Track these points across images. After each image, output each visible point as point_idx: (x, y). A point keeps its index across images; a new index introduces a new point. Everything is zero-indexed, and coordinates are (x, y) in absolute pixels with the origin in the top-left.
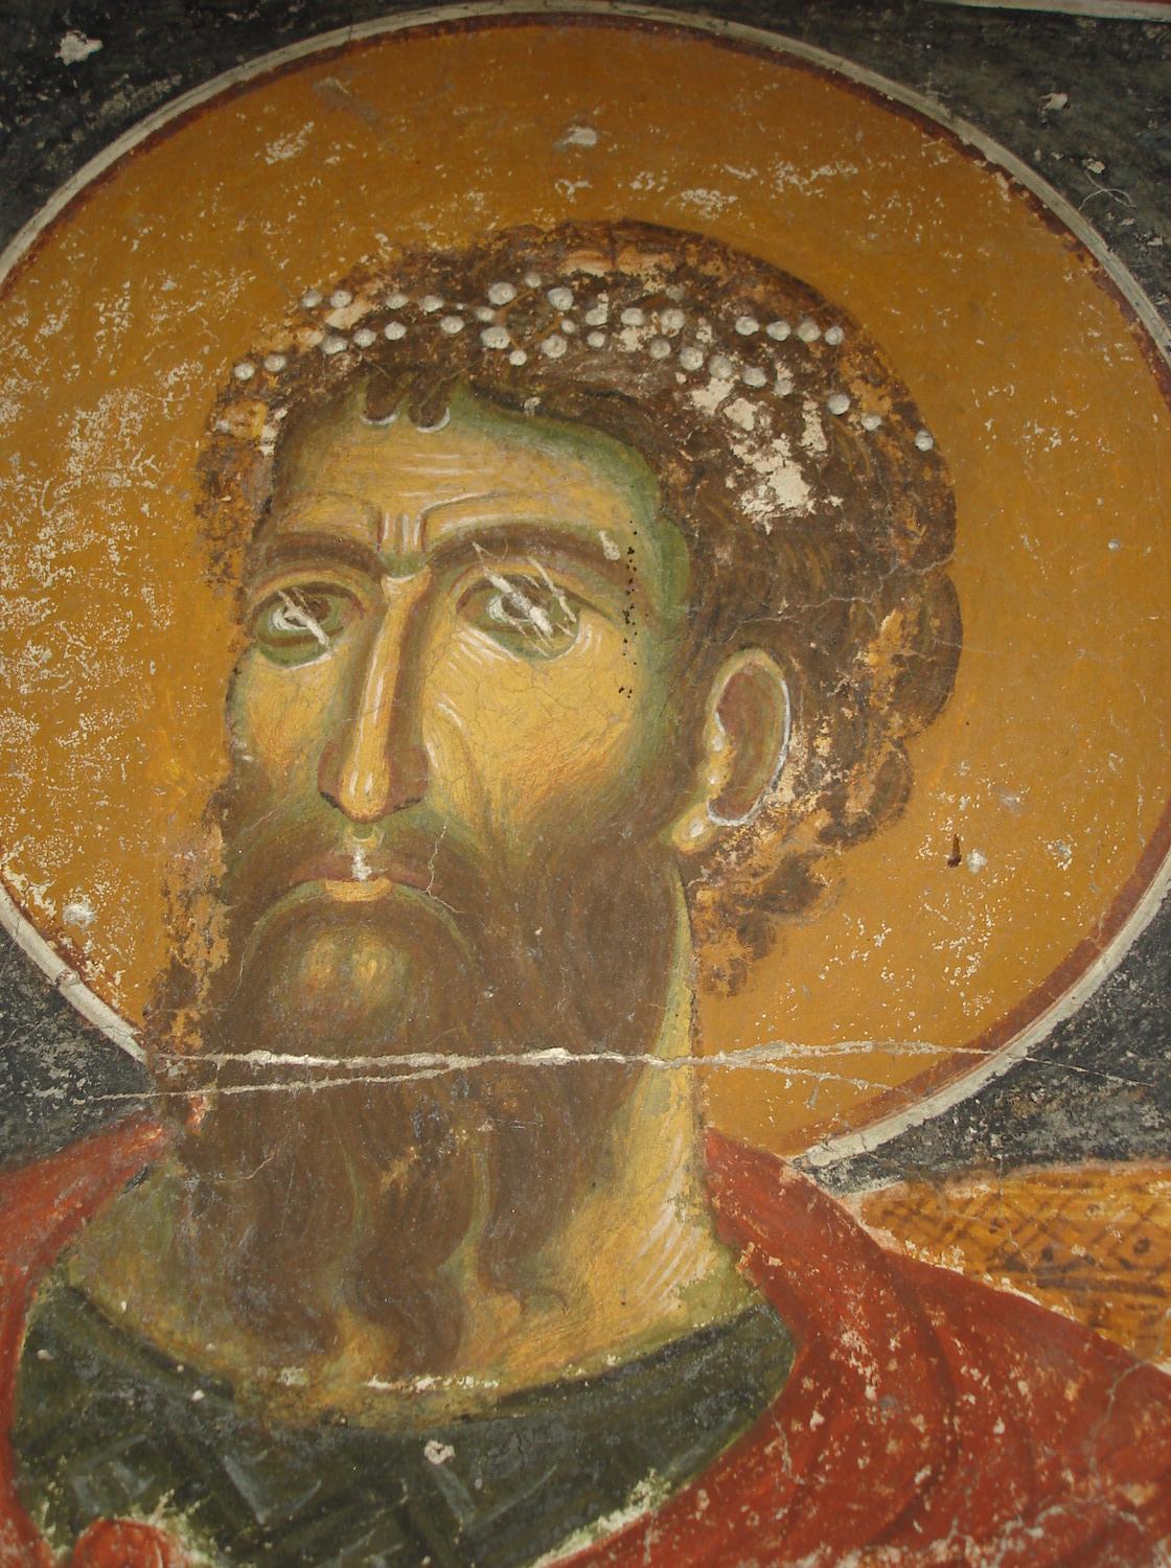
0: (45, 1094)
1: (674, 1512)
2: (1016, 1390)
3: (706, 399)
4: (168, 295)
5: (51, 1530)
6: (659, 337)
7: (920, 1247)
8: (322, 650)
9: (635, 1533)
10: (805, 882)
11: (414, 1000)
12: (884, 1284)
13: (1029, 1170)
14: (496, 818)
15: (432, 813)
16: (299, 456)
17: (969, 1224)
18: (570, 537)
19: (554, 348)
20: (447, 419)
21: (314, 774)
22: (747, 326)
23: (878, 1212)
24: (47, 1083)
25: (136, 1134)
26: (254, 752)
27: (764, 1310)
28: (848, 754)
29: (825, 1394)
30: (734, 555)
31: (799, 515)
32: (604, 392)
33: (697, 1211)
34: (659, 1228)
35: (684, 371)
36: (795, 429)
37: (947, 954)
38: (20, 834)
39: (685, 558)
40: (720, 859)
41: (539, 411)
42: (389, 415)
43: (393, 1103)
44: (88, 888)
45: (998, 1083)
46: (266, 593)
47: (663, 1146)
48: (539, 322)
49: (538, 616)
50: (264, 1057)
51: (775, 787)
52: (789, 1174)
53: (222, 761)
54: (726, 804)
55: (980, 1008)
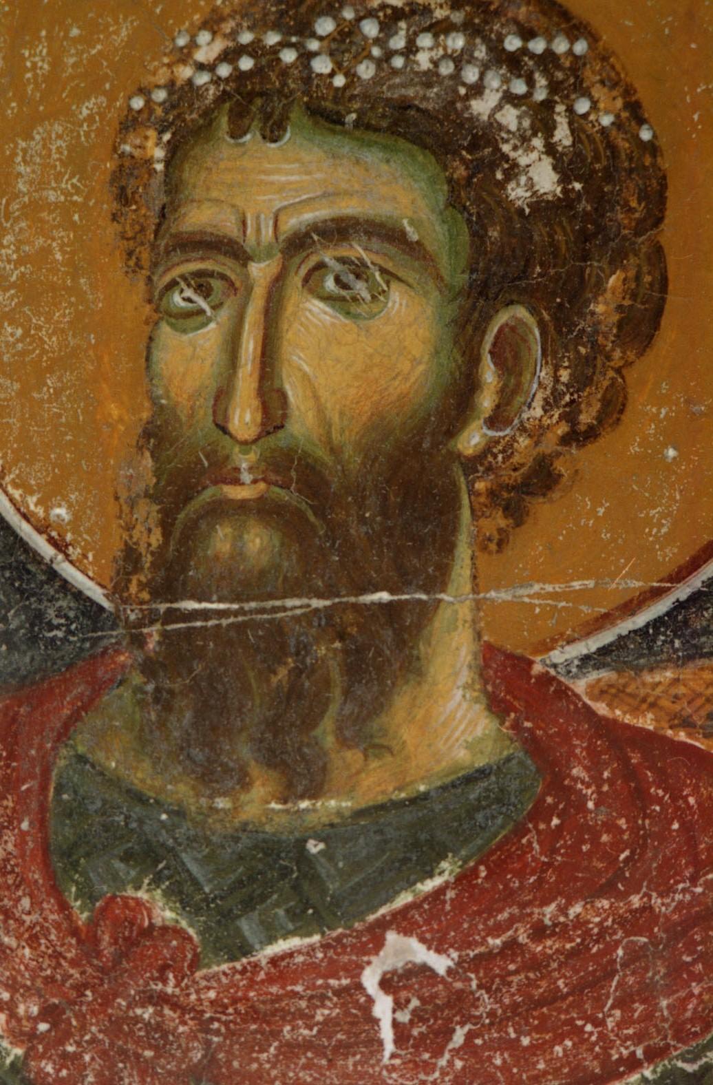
0: (51, 634)
1: (465, 879)
2: (687, 803)
3: (481, 107)
4: (75, 40)
5: (79, 903)
6: (446, 56)
7: (625, 713)
8: (209, 320)
9: (440, 892)
10: (550, 474)
11: (286, 564)
12: (600, 737)
13: (700, 662)
14: (335, 435)
15: (292, 436)
16: (182, 171)
17: (659, 698)
18: (382, 225)
19: (366, 71)
20: (288, 135)
21: (210, 411)
22: (513, 43)
23: (596, 691)
24: (51, 627)
25: (112, 657)
26: (168, 398)
27: (521, 755)
28: (582, 381)
29: (561, 806)
30: (501, 232)
31: (550, 198)
32: (404, 106)
33: (476, 694)
34: (451, 705)
35: (464, 84)
36: (548, 128)
37: (648, 522)
38: (15, 462)
39: (465, 237)
40: (490, 459)
41: (357, 124)
42: (245, 133)
43: (277, 629)
44: (65, 498)
45: (680, 606)
46: (167, 279)
47: (452, 656)
48: (354, 49)
49: (361, 288)
50: (191, 605)
51: (529, 407)
52: (537, 668)
53: (147, 404)
54: (493, 421)
55: (671, 556)
